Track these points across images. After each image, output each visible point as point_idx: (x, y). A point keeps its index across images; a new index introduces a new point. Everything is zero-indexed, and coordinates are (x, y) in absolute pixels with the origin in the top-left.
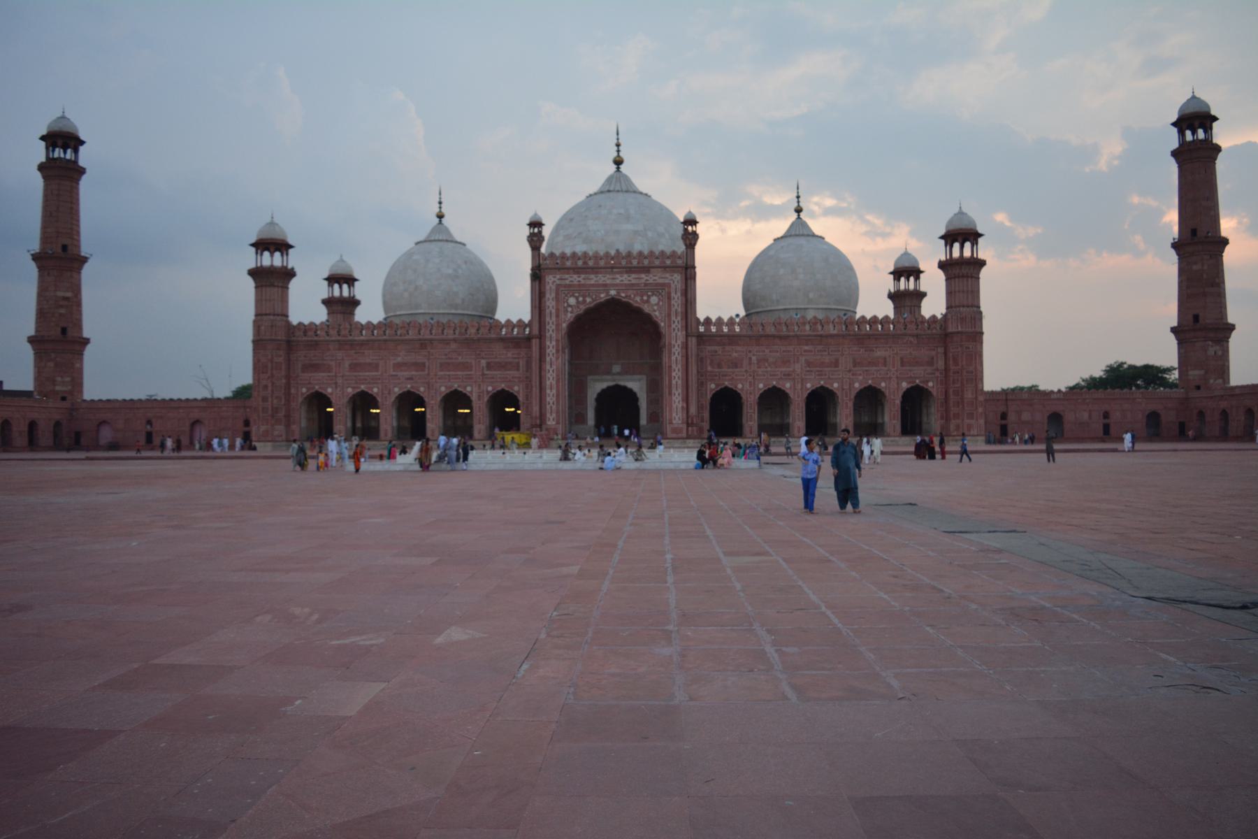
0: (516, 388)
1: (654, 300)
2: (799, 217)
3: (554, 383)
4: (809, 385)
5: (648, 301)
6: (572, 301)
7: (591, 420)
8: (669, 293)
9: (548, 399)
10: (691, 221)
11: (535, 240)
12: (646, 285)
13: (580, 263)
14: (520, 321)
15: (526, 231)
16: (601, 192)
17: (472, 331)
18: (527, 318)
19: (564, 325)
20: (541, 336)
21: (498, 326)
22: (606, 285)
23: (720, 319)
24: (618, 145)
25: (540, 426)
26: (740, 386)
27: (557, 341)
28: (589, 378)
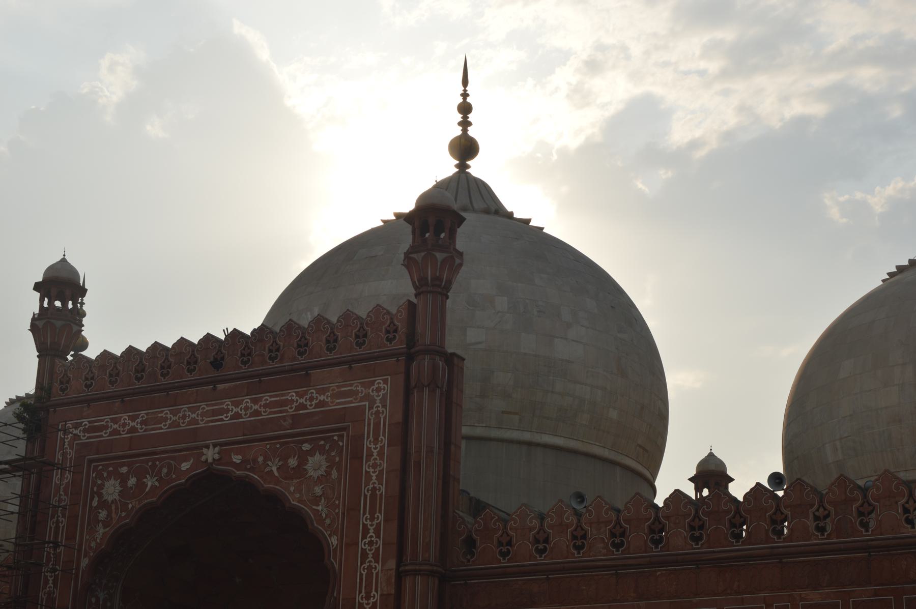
1: (316, 464)
5: (300, 471)
6: (111, 490)
19: (85, 562)
24: (465, 109)
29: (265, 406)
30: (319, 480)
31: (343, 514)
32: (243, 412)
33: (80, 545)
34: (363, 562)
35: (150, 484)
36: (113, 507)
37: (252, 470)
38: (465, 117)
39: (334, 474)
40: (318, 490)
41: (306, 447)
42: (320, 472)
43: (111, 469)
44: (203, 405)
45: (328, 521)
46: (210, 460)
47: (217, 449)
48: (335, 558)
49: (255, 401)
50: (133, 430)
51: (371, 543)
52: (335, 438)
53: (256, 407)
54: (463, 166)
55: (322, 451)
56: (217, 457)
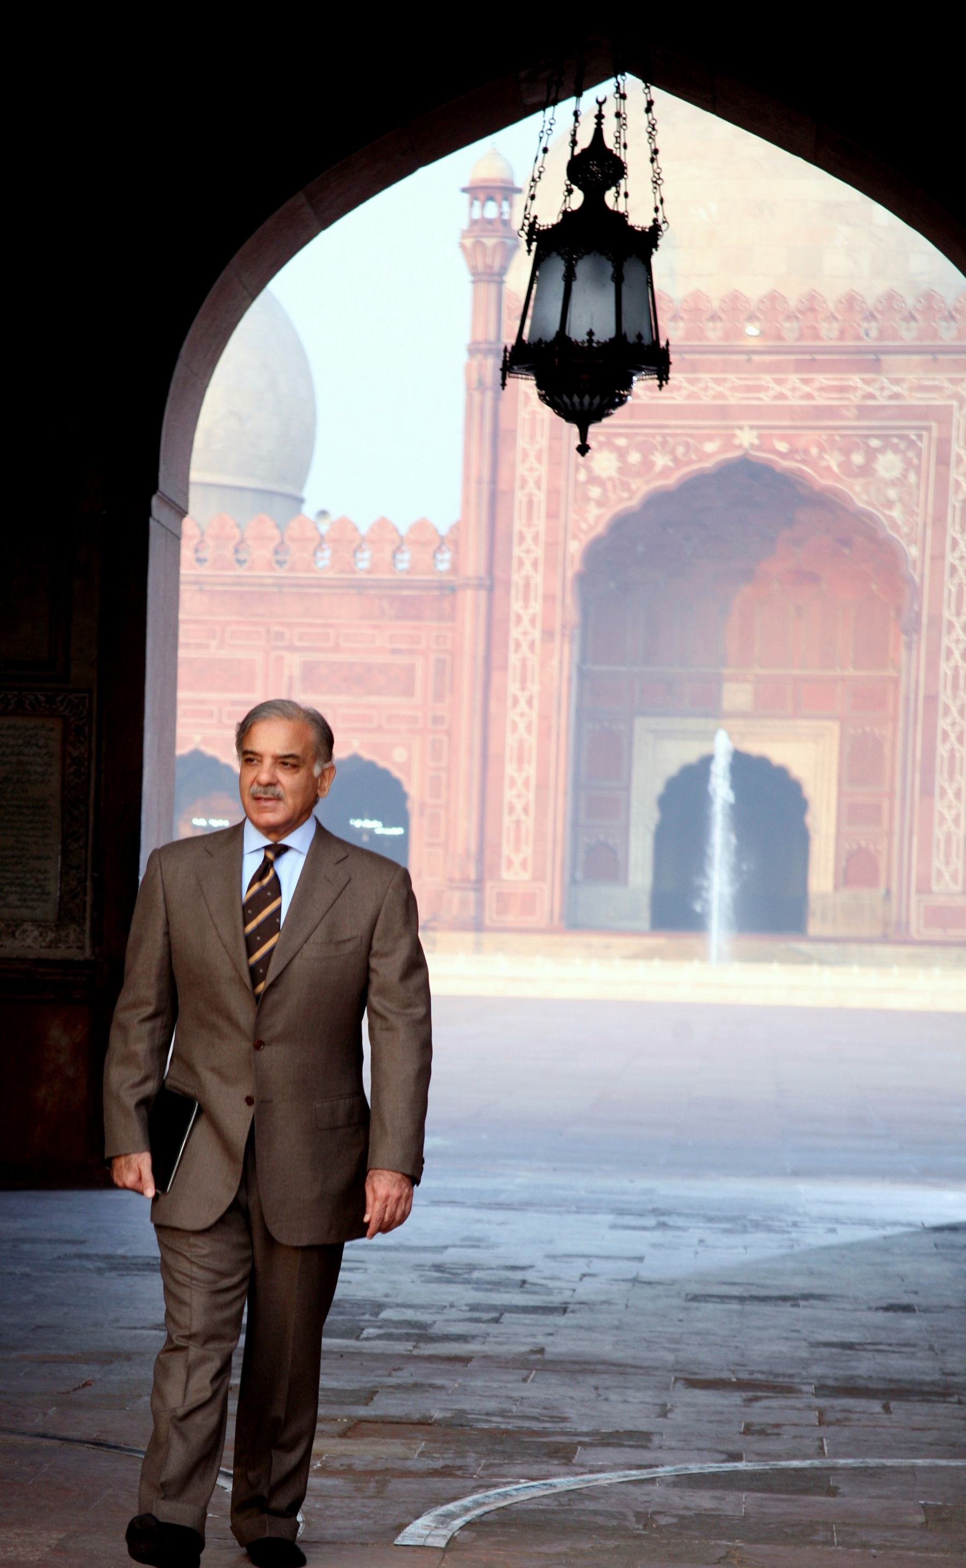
1: (888, 465)
3: (532, 740)
5: (866, 470)
8: (944, 444)
9: (509, 795)
12: (863, 412)
14: (422, 525)
17: (261, 553)
20: (493, 583)
22: (723, 412)
25: (479, 885)
27: (549, 598)
28: (641, 724)
30: (893, 483)
31: (925, 524)
32: (789, 394)
36: (609, 485)
37: (803, 461)
39: (912, 478)
40: (892, 494)
41: (875, 443)
42: (896, 473)
43: (602, 439)
44: (731, 376)
45: (905, 530)
47: (755, 433)
48: (914, 569)
49: (805, 381)
52: (914, 437)
55: (896, 449)
56: (756, 442)
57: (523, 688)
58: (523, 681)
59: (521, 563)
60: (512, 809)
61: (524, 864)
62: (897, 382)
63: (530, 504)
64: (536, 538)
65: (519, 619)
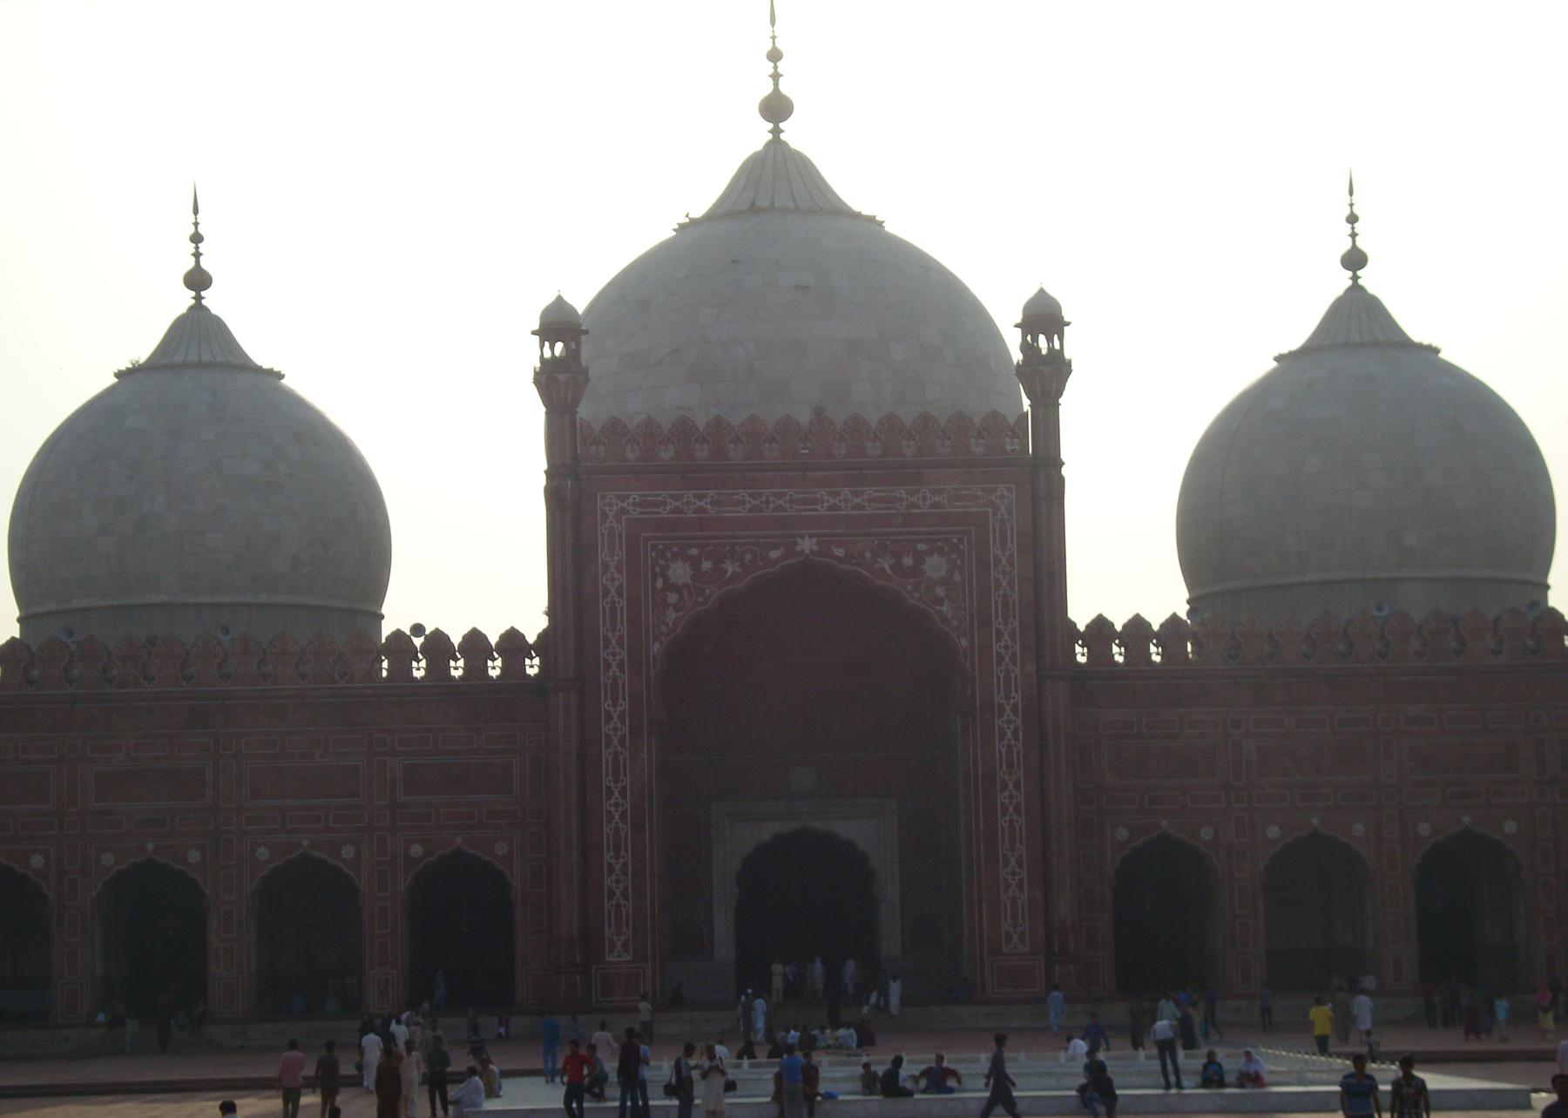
0: (501, 848)
2: (1355, 278)
4: (1424, 829)
6: (680, 572)
7: (724, 947)
9: (607, 881)
10: (1043, 317)
11: (558, 384)
13: (702, 453)
15: (530, 354)
16: (723, 212)
18: (533, 624)
19: (656, 647)
21: (438, 645)
23: (1137, 625)
24: (775, 56)
26: (1207, 833)
29: (869, 500)
33: (647, 630)
34: (999, 665)
35: (730, 570)
38: (776, 68)
39: (957, 577)
40: (940, 591)
45: (955, 623)
46: (807, 551)
47: (814, 540)
49: (855, 494)
50: (700, 510)
51: (1006, 647)
53: (858, 500)
54: (776, 132)
56: (815, 548)
57: (616, 782)
58: (616, 773)
59: (608, 666)
60: (612, 894)
61: (625, 946)
62: (939, 492)
63: (613, 609)
64: (620, 640)
65: (609, 716)
